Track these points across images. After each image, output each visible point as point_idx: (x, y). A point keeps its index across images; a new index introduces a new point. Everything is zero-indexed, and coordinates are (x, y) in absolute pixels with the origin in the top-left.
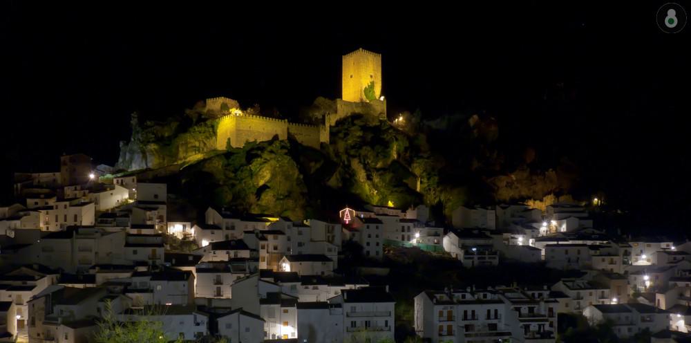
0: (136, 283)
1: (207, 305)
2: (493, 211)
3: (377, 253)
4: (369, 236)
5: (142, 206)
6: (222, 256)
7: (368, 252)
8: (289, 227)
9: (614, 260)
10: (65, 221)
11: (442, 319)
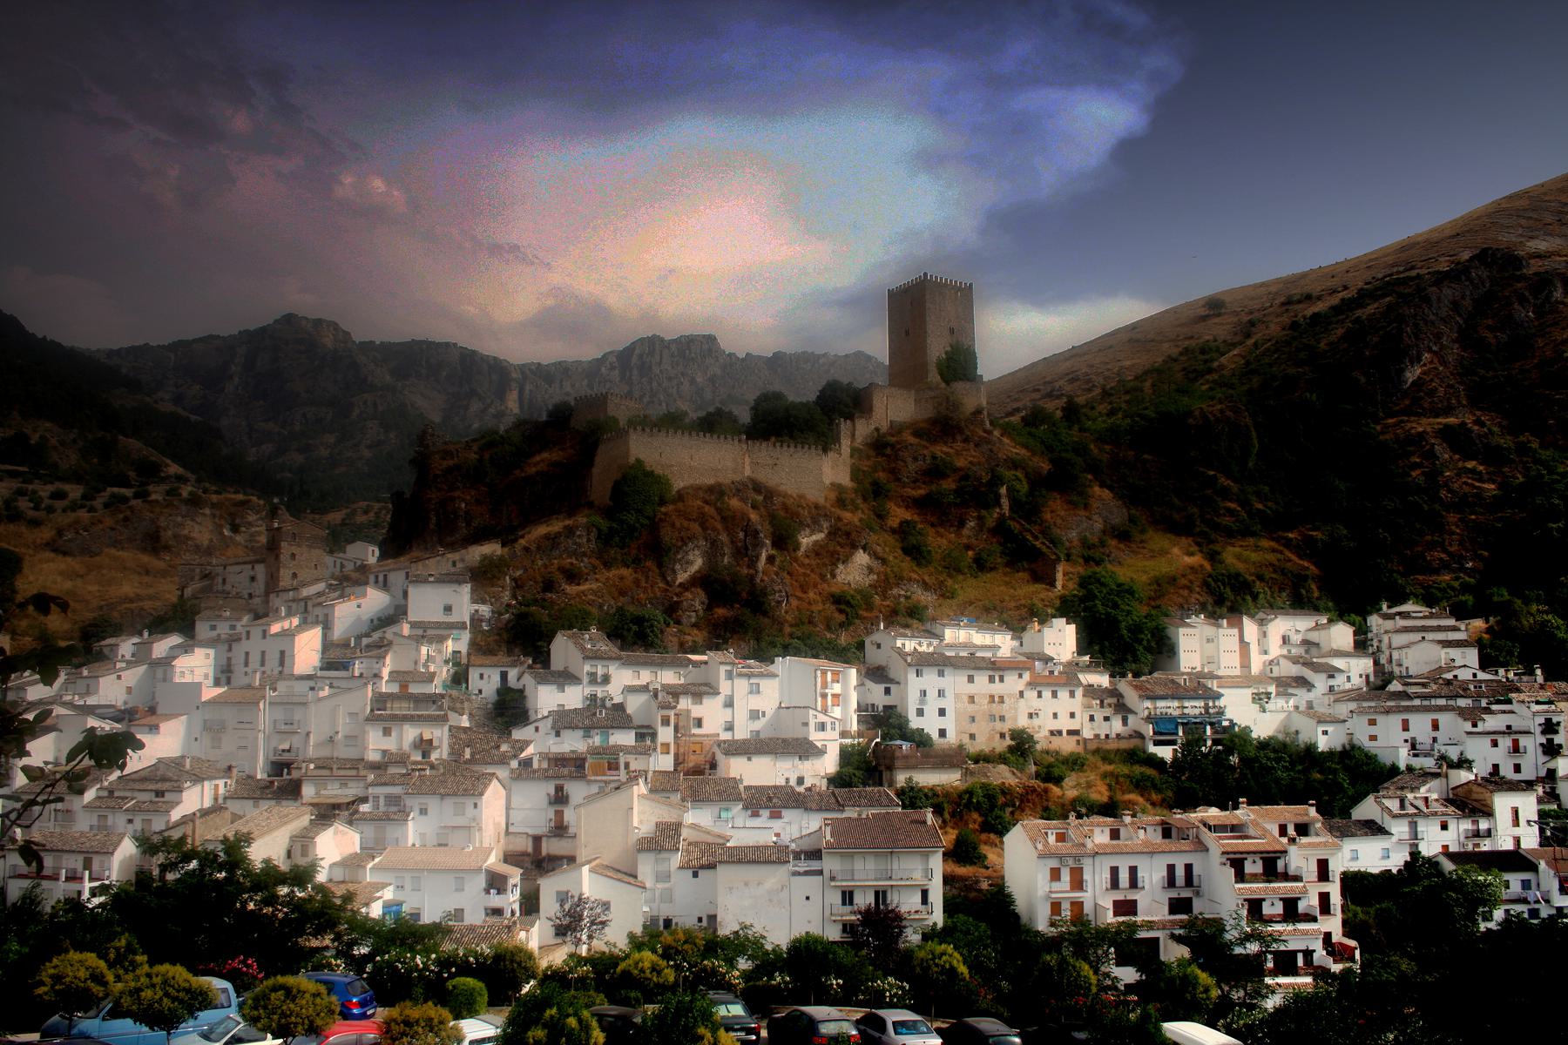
0: (376, 798)
2: (1235, 631)
6: (573, 743)
8: (730, 676)
9: (1521, 744)
10: (263, 664)
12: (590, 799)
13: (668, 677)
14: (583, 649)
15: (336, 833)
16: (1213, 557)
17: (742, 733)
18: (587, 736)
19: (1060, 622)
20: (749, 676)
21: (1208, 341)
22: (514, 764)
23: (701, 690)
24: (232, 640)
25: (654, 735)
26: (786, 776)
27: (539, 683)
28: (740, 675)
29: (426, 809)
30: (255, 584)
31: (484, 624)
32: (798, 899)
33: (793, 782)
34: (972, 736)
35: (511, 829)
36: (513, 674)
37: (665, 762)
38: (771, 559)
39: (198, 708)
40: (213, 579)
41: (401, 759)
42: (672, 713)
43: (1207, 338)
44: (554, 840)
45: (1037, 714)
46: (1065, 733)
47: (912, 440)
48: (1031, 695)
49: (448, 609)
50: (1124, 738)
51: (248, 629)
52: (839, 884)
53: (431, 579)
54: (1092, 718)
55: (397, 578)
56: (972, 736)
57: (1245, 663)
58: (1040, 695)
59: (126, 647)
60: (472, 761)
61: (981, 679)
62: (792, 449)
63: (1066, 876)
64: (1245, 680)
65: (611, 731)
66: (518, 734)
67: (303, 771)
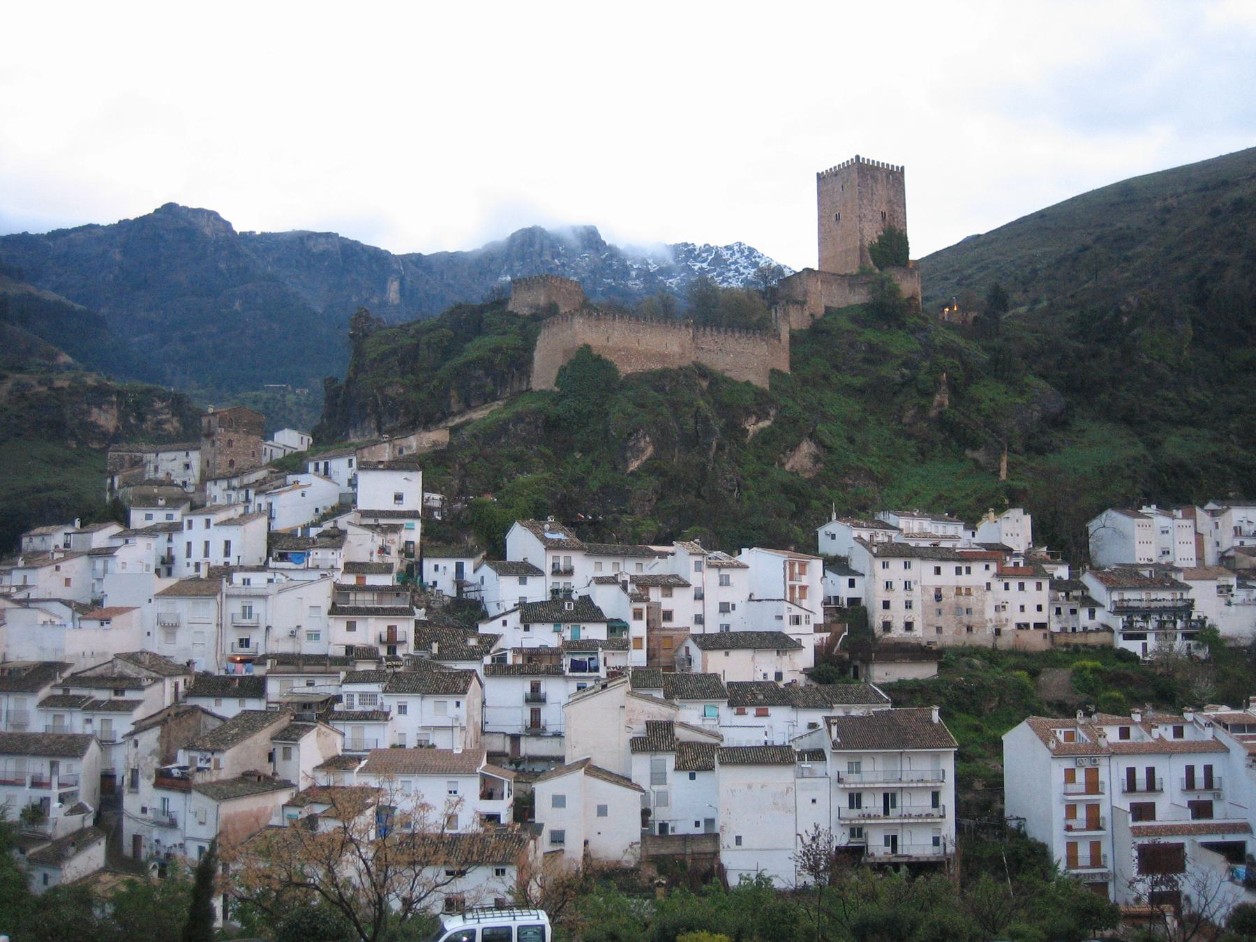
0: (350, 696)
1: (508, 750)
2: (1189, 522)
3: (909, 626)
4: (888, 585)
5: (371, 521)
6: (544, 636)
7: (887, 626)
10: (207, 554)
11: (1071, 788)
12: (574, 700)
13: (629, 568)
14: (544, 540)
15: (318, 735)
16: (1153, 446)
17: (712, 627)
18: (557, 631)
19: (1017, 513)
20: (719, 567)
21: (1121, 229)
22: (487, 660)
23: (670, 584)
24: (173, 529)
25: (625, 627)
26: (763, 671)
27: (500, 575)
28: (710, 566)
29: (405, 707)
30: (189, 472)
31: (436, 513)
32: (804, 799)
33: (771, 678)
34: (939, 630)
35: (487, 729)
36: (469, 565)
37: (638, 658)
38: (720, 447)
39: (150, 600)
40: (144, 466)
41: (368, 653)
42: (643, 606)
43: (1119, 225)
44: (533, 740)
45: (1004, 607)
46: (1032, 626)
47: (850, 326)
48: (998, 585)
49: (399, 497)
50: (1091, 631)
51: (190, 518)
52: (847, 786)
53: (381, 466)
54: (1058, 611)
55: (341, 467)
56: (939, 630)
57: (1200, 557)
58: (1007, 587)
59: (58, 537)
60: (440, 656)
61: (948, 568)
62: (737, 335)
63: (1080, 776)
64: (1202, 571)
65: (582, 625)
66: (484, 628)
67: (268, 667)
